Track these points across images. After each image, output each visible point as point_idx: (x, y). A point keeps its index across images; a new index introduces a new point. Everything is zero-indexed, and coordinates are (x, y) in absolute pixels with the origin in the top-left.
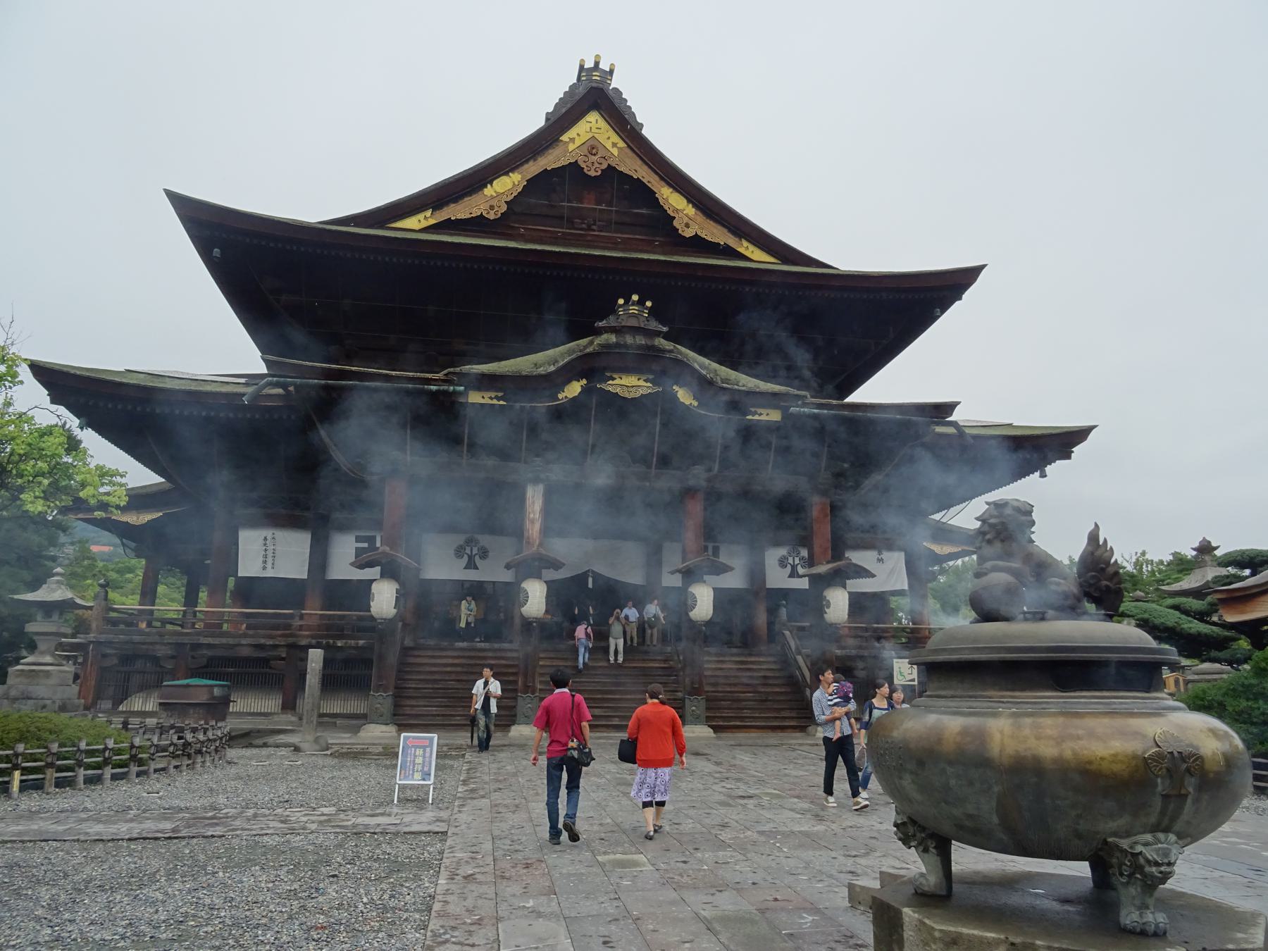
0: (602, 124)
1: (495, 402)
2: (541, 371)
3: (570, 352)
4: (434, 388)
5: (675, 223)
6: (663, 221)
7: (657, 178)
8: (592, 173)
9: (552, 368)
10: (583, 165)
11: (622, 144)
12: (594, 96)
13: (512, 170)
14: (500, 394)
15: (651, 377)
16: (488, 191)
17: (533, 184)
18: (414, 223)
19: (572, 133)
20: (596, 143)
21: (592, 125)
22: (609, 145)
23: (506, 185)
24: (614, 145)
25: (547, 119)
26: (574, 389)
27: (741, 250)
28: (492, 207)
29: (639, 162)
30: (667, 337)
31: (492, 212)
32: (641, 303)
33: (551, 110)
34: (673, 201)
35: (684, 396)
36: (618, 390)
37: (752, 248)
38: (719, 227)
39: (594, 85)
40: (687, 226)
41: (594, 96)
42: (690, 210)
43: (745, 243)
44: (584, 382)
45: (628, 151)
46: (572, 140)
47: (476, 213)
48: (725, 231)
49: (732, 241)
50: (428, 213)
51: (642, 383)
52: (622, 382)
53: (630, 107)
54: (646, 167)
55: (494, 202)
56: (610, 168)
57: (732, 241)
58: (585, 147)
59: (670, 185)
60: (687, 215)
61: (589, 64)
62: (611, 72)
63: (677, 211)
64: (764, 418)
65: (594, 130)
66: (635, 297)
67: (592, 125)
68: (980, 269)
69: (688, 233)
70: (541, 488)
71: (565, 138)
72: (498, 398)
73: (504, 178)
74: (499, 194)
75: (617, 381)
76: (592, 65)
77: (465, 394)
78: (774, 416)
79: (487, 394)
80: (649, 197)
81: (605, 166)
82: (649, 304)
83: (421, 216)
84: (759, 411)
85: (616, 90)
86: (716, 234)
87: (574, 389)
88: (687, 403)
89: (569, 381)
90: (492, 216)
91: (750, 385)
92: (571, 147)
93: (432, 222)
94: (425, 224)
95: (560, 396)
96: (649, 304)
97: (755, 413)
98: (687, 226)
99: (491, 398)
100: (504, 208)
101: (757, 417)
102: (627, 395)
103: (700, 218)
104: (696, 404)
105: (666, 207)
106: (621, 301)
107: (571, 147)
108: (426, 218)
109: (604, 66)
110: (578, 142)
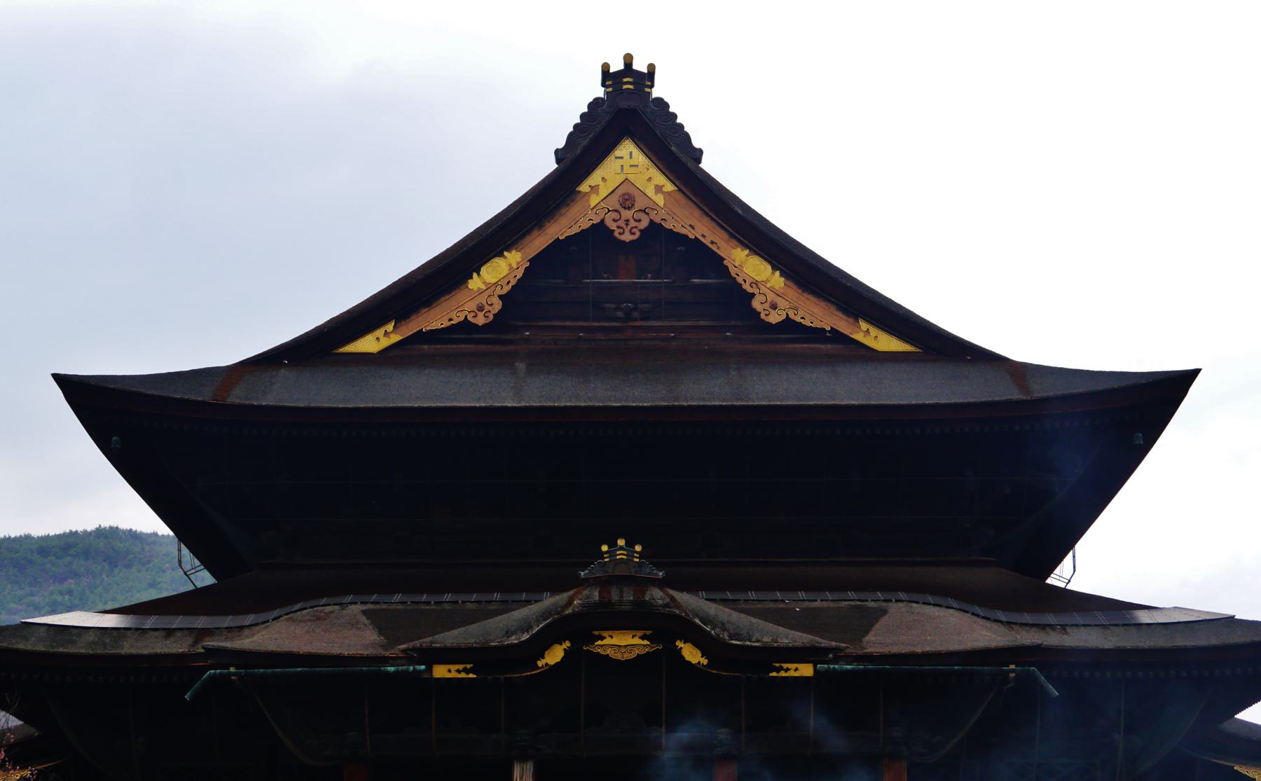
0: (640, 158)
1: (463, 675)
2: (513, 640)
3: (544, 615)
4: (391, 669)
5: (756, 304)
6: (737, 298)
7: (726, 236)
8: (627, 237)
9: (525, 637)
10: (612, 226)
11: (669, 187)
12: (628, 111)
13: (508, 249)
14: (469, 666)
15: (648, 632)
16: (475, 283)
17: (536, 265)
18: (369, 344)
19: (595, 178)
20: (632, 190)
21: (628, 164)
22: (650, 192)
23: (501, 271)
24: (659, 189)
25: (558, 161)
26: (555, 655)
27: (859, 337)
28: (481, 308)
29: (697, 212)
30: (662, 584)
31: (481, 314)
32: (631, 544)
33: (561, 144)
34: (751, 268)
35: (692, 654)
36: (609, 652)
37: (874, 331)
38: (823, 304)
39: (624, 104)
40: (774, 307)
41: (628, 111)
42: (777, 280)
43: (864, 325)
44: (567, 644)
45: (679, 196)
46: (594, 189)
48: (833, 308)
49: (843, 325)
50: (390, 327)
51: (637, 641)
52: (615, 641)
53: (681, 126)
54: (706, 220)
55: (482, 300)
56: (655, 231)
57: (843, 325)
58: (615, 197)
59: (745, 246)
60: (772, 290)
61: (617, 66)
62: (651, 74)
63: (755, 283)
64: (792, 673)
65: (627, 169)
66: (621, 542)
67: (628, 164)
68: (1192, 375)
69: (774, 318)
70: (530, 767)
71: (584, 188)
72: (465, 670)
73: (498, 261)
74: (489, 286)
75: (607, 641)
76: (621, 67)
77: (429, 669)
78: (806, 670)
79: (454, 667)
80: (717, 264)
81: (644, 224)
82: (638, 548)
83: (380, 333)
84: (785, 666)
85: (662, 104)
86: (816, 314)
87: (555, 655)
88: (694, 661)
89: (548, 646)
90: (480, 320)
91: (766, 639)
92: (594, 200)
93: (395, 338)
94: (385, 343)
95: (540, 663)
96: (638, 548)
97: (779, 669)
98: (774, 307)
99: (458, 671)
100: (498, 305)
101: (782, 674)
102: (619, 656)
103: (793, 293)
104: (705, 661)
105: (740, 280)
106: (605, 548)
107: (594, 200)
109: (640, 66)
110: (604, 192)
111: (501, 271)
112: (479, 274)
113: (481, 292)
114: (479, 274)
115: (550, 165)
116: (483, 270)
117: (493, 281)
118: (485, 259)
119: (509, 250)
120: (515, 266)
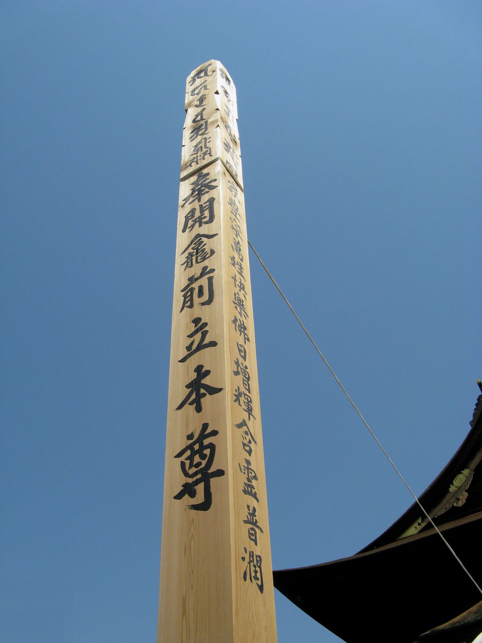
16: (452, 489)
17: (478, 472)
18: (413, 531)
23: (462, 479)
25: (472, 426)
33: (471, 419)
47: (449, 507)
50: (420, 521)
74: (459, 488)
83: (416, 525)
94: (420, 528)
108: (419, 524)
111: (462, 479)
112: (453, 485)
113: (456, 492)
114: (453, 485)
115: (469, 428)
116: (454, 482)
117: (460, 485)
118: (454, 477)
119: (463, 470)
120: (468, 475)
